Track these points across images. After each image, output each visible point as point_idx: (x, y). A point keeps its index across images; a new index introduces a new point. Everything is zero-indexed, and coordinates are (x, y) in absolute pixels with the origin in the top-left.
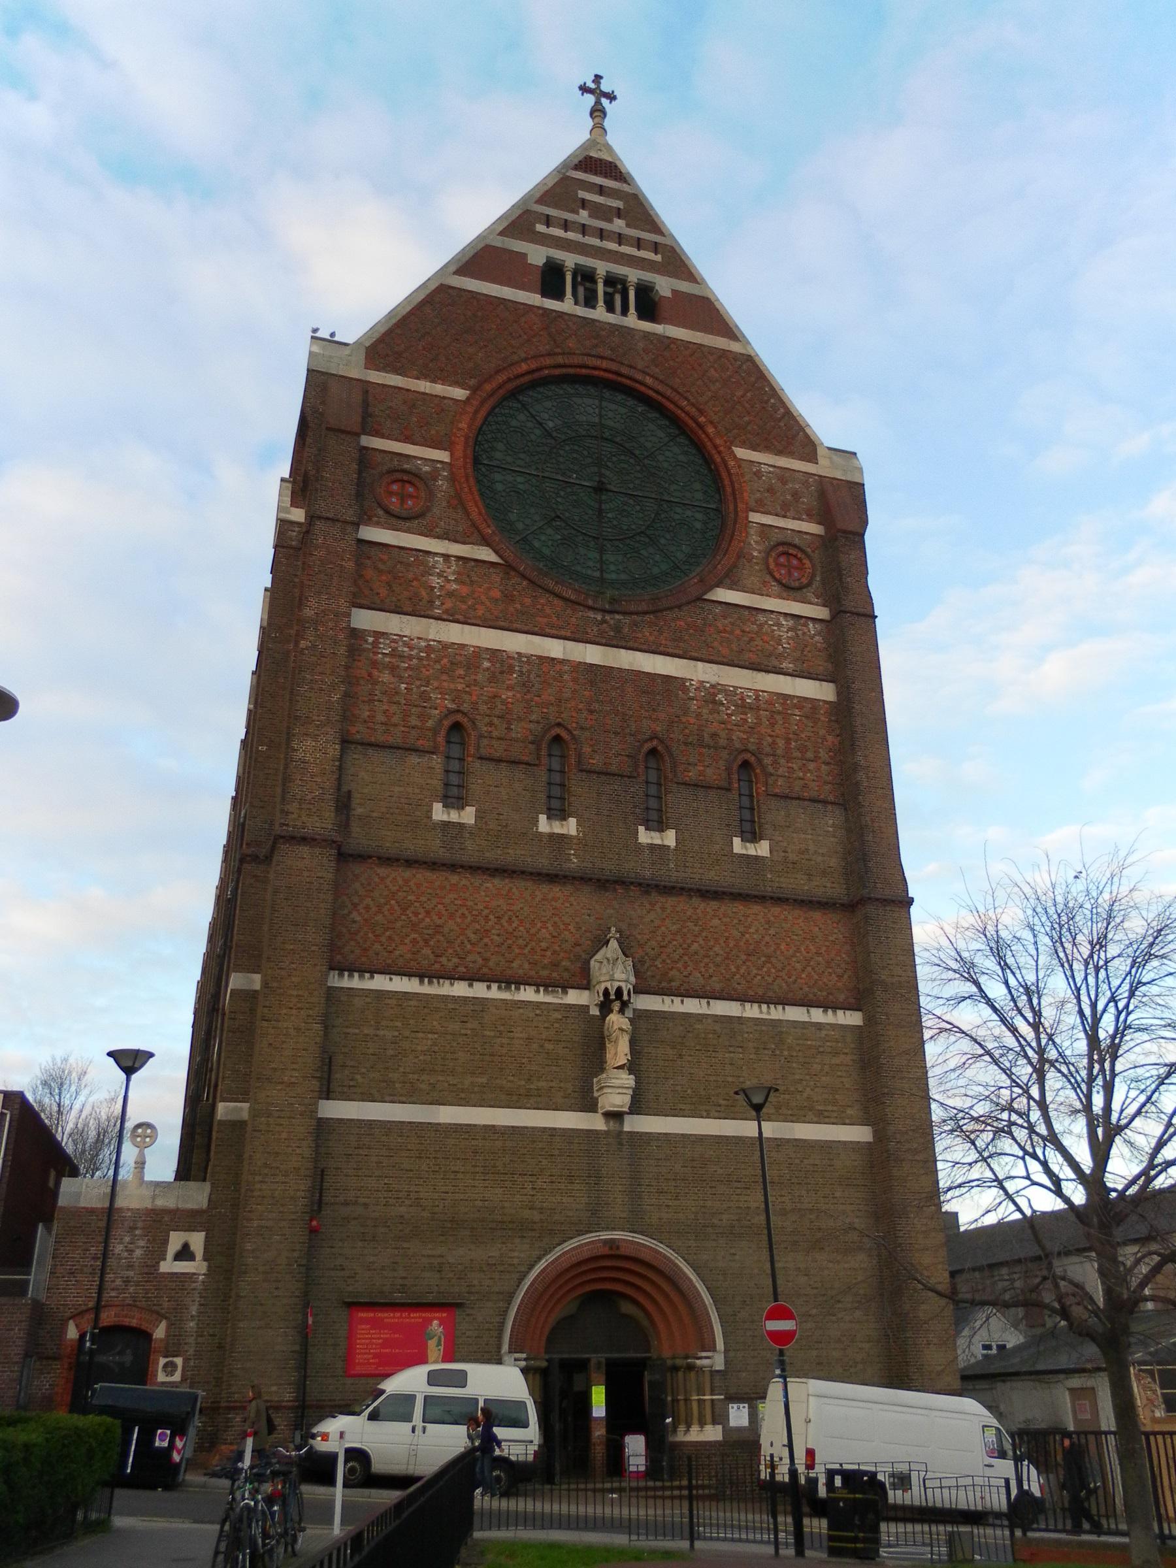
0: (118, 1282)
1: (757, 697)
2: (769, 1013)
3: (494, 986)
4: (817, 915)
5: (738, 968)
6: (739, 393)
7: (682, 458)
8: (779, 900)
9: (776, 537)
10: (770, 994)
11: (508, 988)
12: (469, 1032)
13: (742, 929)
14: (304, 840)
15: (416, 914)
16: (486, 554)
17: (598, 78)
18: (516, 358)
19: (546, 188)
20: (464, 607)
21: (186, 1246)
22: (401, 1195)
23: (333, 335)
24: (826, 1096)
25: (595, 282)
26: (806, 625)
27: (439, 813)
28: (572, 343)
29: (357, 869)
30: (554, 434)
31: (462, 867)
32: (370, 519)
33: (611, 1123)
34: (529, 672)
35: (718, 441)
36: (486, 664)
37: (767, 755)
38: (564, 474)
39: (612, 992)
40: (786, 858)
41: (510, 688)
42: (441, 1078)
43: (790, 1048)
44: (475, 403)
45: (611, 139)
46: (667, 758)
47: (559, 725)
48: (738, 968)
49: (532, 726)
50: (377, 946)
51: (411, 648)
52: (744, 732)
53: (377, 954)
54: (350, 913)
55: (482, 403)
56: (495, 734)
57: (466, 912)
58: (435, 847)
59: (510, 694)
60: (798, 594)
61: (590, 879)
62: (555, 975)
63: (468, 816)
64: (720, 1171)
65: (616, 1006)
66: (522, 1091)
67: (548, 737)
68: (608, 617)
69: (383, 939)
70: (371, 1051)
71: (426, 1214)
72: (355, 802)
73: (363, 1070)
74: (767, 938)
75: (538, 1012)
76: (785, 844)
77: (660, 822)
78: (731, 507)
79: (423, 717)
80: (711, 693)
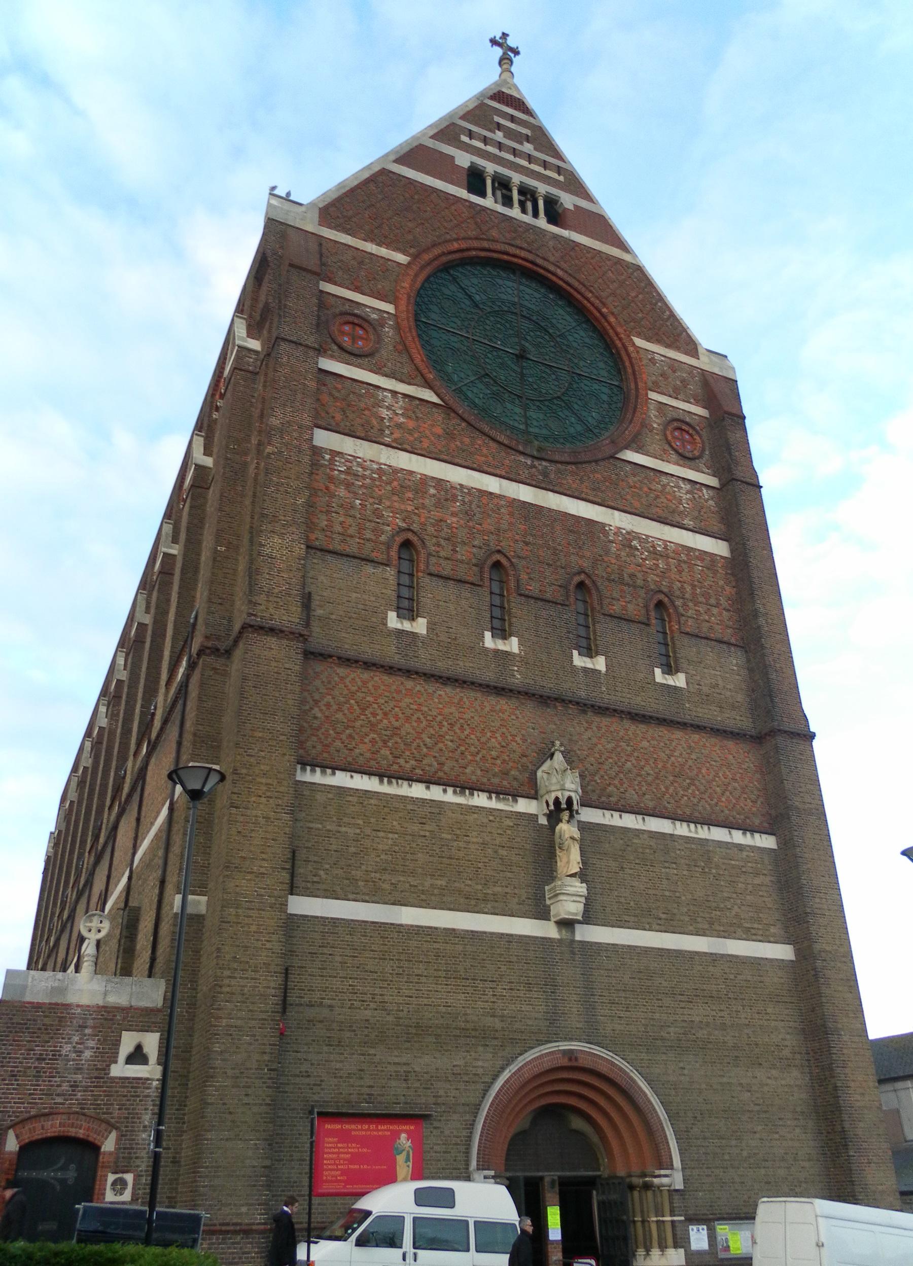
0: (65, 1087)
1: (666, 548)
2: (696, 832)
3: (450, 790)
4: (730, 744)
5: (667, 788)
6: (633, 294)
7: (587, 340)
8: (698, 728)
9: (671, 414)
10: (697, 814)
11: (462, 793)
12: (427, 834)
13: (668, 752)
14: (272, 631)
15: (374, 715)
16: (429, 395)
17: (505, 35)
18: (448, 237)
19: (468, 109)
20: (411, 438)
21: (139, 1048)
22: (365, 998)
23: (288, 194)
24: (751, 914)
25: (510, 190)
26: (701, 491)
28: (494, 233)
29: (319, 667)
30: (481, 306)
31: (417, 673)
32: (325, 352)
33: (564, 932)
34: (471, 502)
35: (619, 330)
36: (432, 491)
37: (678, 597)
38: (490, 340)
39: (563, 801)
40: (700, 690)
41: (454, 514)
42: (402, 879)
43: (717, 867)
44: (415, 268)
45: (517, 80)
46: (594, 592)
47: (499, 552)
48: (667, 788)
49: (474, 550)
50: (338, 743)
51: (364, 469)
52: (657, 575)
53: (338, 751)
54: (312, 709)
55: (423, 268)
56: (442, 554)
57: (421, 717)
58: (391, 653)
59: (455, 519)
60: (692, 463)
61: (534, 695)
62: (505, 783)
63: (420, 626)
64: (665, 984)
65: (565, 815)
66: (480, 895)
67: (489, 562)
68: (536, 463)
69: (344, 737)
70: (334, 847)
71: (390, 1018)
72: (314, 604)
73: (327, 866)
74: (690, 762)
75: (491, 818)
76: (698, 678)
77: (589, 649)
78: (633, 386)
79: (377, 532)
80: (628, 539)
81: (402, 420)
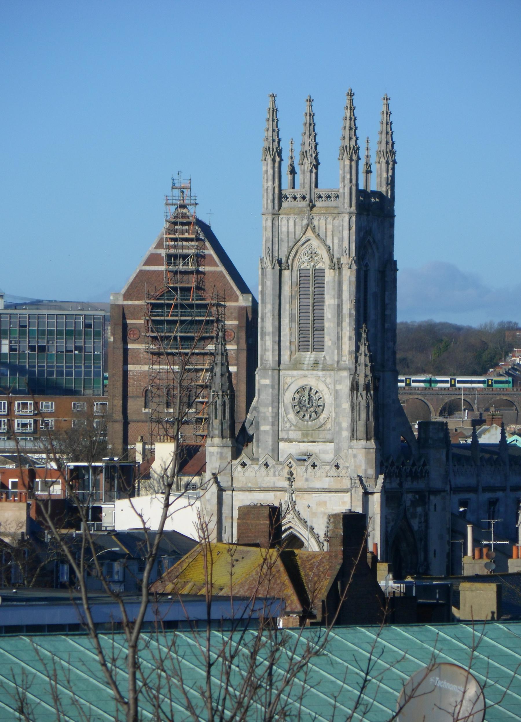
27: (144, 411)
58: (143, 418)
79: (140, 389)
81: (146, 356)
